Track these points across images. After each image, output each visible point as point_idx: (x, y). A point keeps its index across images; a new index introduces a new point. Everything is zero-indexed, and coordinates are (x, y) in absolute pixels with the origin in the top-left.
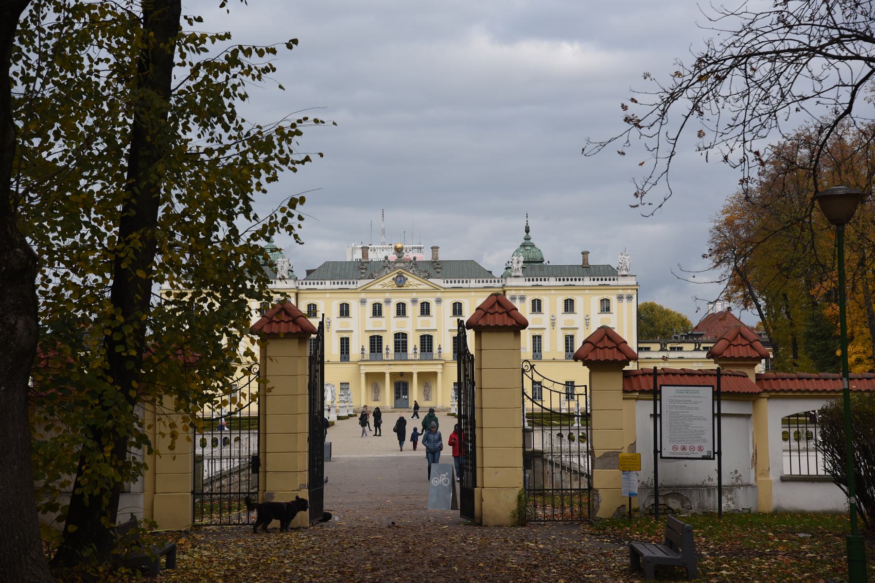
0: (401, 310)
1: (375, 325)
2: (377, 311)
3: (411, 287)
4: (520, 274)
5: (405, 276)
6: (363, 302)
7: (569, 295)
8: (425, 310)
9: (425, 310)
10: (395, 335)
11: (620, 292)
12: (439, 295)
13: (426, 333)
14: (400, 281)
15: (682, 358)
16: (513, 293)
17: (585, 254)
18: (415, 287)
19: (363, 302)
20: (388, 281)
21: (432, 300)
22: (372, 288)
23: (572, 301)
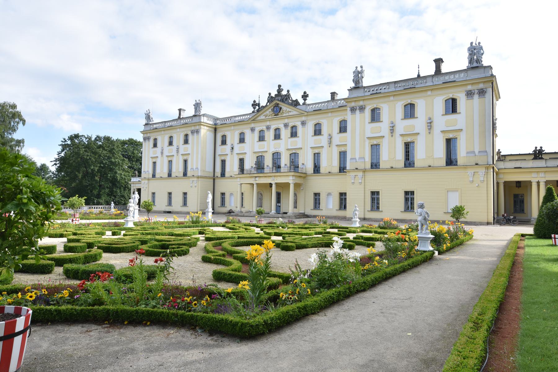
1: (259, 147)
2: (262, 138)
3: (284, 115)
5: (280, 106)
8: (294, 134)
9: (294, 134)
12: (303, 119)
13: (294, 151)
14: (277, 110)
16: (353, 104)
17: (438, 62)
18: (287, 114)
19: (253, 130)
20: (269, 112)
21: (298, 124)
22: (259, 118)
23: (412, 106)
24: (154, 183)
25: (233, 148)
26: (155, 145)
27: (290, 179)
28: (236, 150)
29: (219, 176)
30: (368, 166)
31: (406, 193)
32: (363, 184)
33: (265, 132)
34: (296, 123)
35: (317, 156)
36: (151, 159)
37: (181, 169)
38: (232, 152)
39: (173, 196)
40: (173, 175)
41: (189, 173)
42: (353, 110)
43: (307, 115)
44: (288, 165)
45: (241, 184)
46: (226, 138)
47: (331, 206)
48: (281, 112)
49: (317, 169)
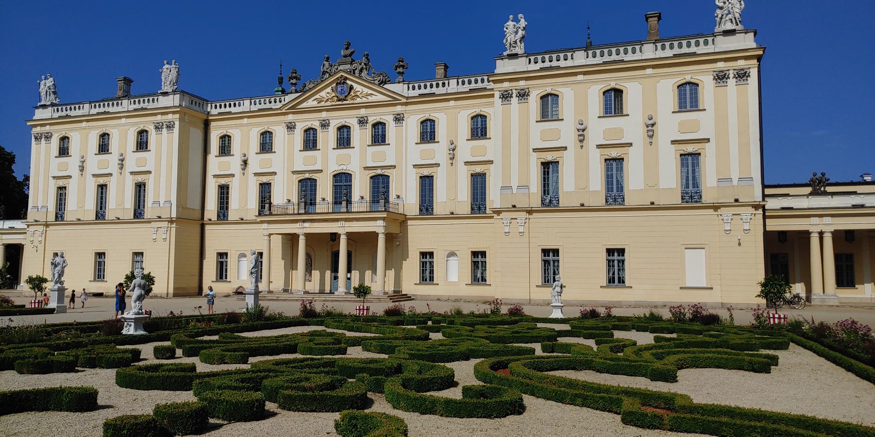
0: (344, 139)
1: (304, 161)
2: (310, 142)
3: (358, 100)
4: (520, 49)
6: (291, 127)
7: (612, 81)
8: (379, 136)
9: (379, 136)
10: (335, 176)
11: (721, 65)
12: (399, 109)
15: (862, 206)
18: (364, 100)
19: (291, 127)
21: (389, 120)
23: (618, 93)
24: (56, 232)
25: (245, 163)
26: (64, 151)
27: (378, 227)
28: (253, 167)
29: (214, 218)
30: (536, 203)
31: (610, 252)
32: (526, 234)
33: (319, 130)
34: (382, 117)
35: (427, 184)
36: (51, 180)
37: (129, 203)
38: (244, 169)
39: (108, 260)
40: (110, 215)
41: (148, 213)
42: (506, 96)
43: (406, 104)
44: (367, 197)
45: (270, 235)
46: (229, 140)
47: (453, 277)
48: (352, 93)
49: (426, 207)
